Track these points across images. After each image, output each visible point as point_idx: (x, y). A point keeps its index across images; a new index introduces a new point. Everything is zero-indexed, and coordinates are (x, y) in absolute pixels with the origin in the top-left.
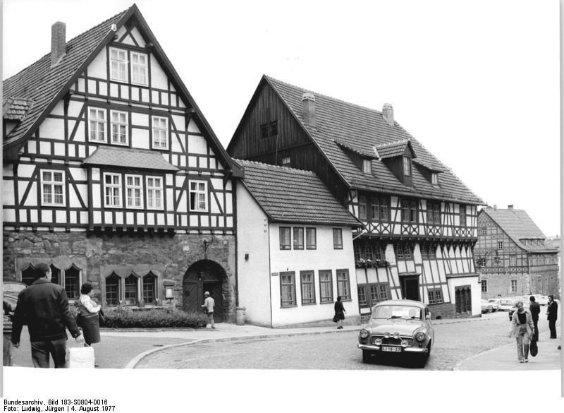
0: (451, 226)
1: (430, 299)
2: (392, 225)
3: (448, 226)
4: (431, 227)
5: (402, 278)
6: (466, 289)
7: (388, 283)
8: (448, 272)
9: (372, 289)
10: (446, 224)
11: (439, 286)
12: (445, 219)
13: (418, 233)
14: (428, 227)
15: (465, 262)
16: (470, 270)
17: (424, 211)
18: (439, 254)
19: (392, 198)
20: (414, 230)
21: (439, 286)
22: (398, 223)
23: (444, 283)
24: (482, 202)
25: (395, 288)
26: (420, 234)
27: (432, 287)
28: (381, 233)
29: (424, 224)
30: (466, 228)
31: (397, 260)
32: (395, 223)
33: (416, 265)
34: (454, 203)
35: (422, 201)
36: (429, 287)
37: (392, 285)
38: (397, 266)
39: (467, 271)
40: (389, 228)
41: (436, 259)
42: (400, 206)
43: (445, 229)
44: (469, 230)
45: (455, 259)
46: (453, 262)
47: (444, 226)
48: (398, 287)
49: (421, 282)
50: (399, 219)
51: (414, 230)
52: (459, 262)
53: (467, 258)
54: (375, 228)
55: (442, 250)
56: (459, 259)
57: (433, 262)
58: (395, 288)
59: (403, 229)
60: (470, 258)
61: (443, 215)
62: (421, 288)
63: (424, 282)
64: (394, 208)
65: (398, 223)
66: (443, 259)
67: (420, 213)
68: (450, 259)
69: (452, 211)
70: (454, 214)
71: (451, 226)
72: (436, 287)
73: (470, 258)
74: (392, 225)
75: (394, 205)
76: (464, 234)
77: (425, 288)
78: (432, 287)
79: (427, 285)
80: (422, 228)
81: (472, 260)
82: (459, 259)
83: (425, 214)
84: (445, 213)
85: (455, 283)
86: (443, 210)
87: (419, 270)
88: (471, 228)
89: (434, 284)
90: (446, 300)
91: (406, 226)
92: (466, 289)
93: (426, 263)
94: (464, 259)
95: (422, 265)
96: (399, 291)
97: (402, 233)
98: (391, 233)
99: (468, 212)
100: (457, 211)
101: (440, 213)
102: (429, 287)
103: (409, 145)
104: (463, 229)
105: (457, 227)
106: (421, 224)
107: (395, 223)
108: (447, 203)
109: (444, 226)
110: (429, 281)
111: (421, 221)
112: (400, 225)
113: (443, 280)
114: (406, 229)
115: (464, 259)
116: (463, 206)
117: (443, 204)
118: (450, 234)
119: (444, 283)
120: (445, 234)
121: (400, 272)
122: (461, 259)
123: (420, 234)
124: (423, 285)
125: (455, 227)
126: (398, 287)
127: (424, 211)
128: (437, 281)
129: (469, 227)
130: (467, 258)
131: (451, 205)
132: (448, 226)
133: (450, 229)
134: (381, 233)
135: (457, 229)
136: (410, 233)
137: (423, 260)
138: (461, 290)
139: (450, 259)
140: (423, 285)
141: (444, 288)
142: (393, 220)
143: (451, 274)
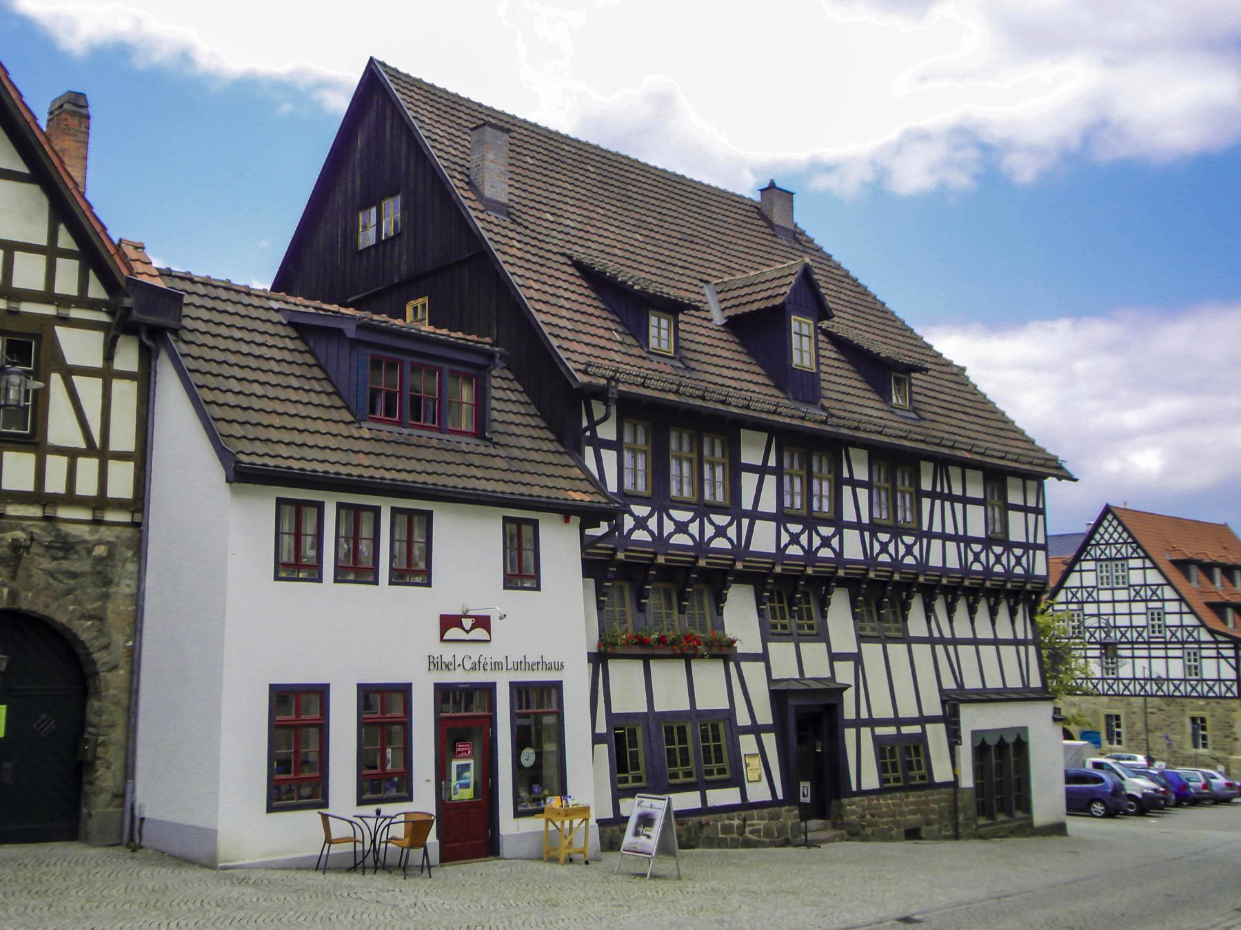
0: (955, 538)
1: (882, 768)
2: (745, 522)
3: (944, 537)
4: (884, 537)
5: (779, 696)
6: (1010, 739)
7: (730, 714)
8: (949, 683)
9: (669, 731)
10: (937, 528)
11: (916, 729)
12: (935, 515)
13: (839, 554)
14: (873, 536)
15: (1008, 652)
16: (1025, 677)
17: (861, 484)
18: (916, 624)
19: (745, 434)
20: (826, 542)
21: (916, 729)
22: (766, 517)
23: (933, 720)
24: (1060, 468)
25: (756, 729)
26: (847, 555)
27: (891, 730)
28: (701, 546)
29: (858, 526)
30: (1009, 546)
31: (768, 635)
32: (755, 515)
33: (834, 657)
34: (965, 465)
35: (853, 452)
36: (880, 731)
37: (743, 719)
38: (764, 657)
39: (1014, 682)
40: (732, 532)
41: (908, 641)
42: (772, 462)
43: (936, 544)
44: (1018, 552)
45: (975, 642)
46: (966, 652)
47: (931, 535)
48: (766, 728)
49: (849, 713)
50: (768, 504)
51: (826, 542)
52: (988, 652)
53: (1015, 642)
54: (681, 527)
55: (929, 610)
56: (986, 642)
57: (897, 651)
58: (756, 729)
59: (785, 538)
60: (1025, 643)
61: (926, 502)
62: (850, 734)
63: (864, 714)
64: (751, 469)
65: (766, 517)
66: (931, 641)
67: (847, 490)
68: (956, 642)
69: (957, 491)
70: (965, 500)
71: (955, 538)
72: (906, 730)
73: (1025, 643)
74: (745, 522)
75: (751, 454)
76: (1000, 562)
77: (866, 732)
78: (891, 730)
79: (872, 722)
80: (851, 537)
81: (1032, 649)
82: (986, 642)
83: (863, 494)
84: (933, 495)
85: (973, 719)
86: (926, 485)
87: (845, 673)
88: (1026, 546)
89: (897, 721)
90: (941, 772)
91: (795, 528)
92: (1010, 739)
93: (872, 652)
94: (1006, 642)
95: (857, 659)
96: (769, 740)
97: (780, 550)
98: (741, 550)
99: (1014, 497)
100: (976, 491)
101: (919, 494)
102: (880, 731)
103: (807, 272)
104: (998, 550)
105: (977, 540)
106: (850, 525)
107: (755, 515)
108: (942, 464)
109: (931, 535)
110: (882, 709)
111: (849, 515)
112: (773, 525)
113: (933, 706)
114: (795, 539)
115: (1006, 642)
116: (996, 477)
117: (927, 469)
118: (953, 562)
119: (933, 720)
120: (935, 561)
121: (774, 677)
122: (996, 642)
123: (846, 555)
124: (858, 723)
125: (968, 540)
126: (766, 728)
127: (861, 484)
128: (908, 709)
129: (1018, 545)
130: (1015, 642)
131: (955, 472)
132: (944, 537)
133: (951, 546)
134: (701, 546)
135: (977, 547)
136: (810, 553)
137: (861, 639)
138: (992, 741)
139: (956, 642)
140: (858, 723)
141: (937, 736)
142: (747, 504)
143: (960, 685)
